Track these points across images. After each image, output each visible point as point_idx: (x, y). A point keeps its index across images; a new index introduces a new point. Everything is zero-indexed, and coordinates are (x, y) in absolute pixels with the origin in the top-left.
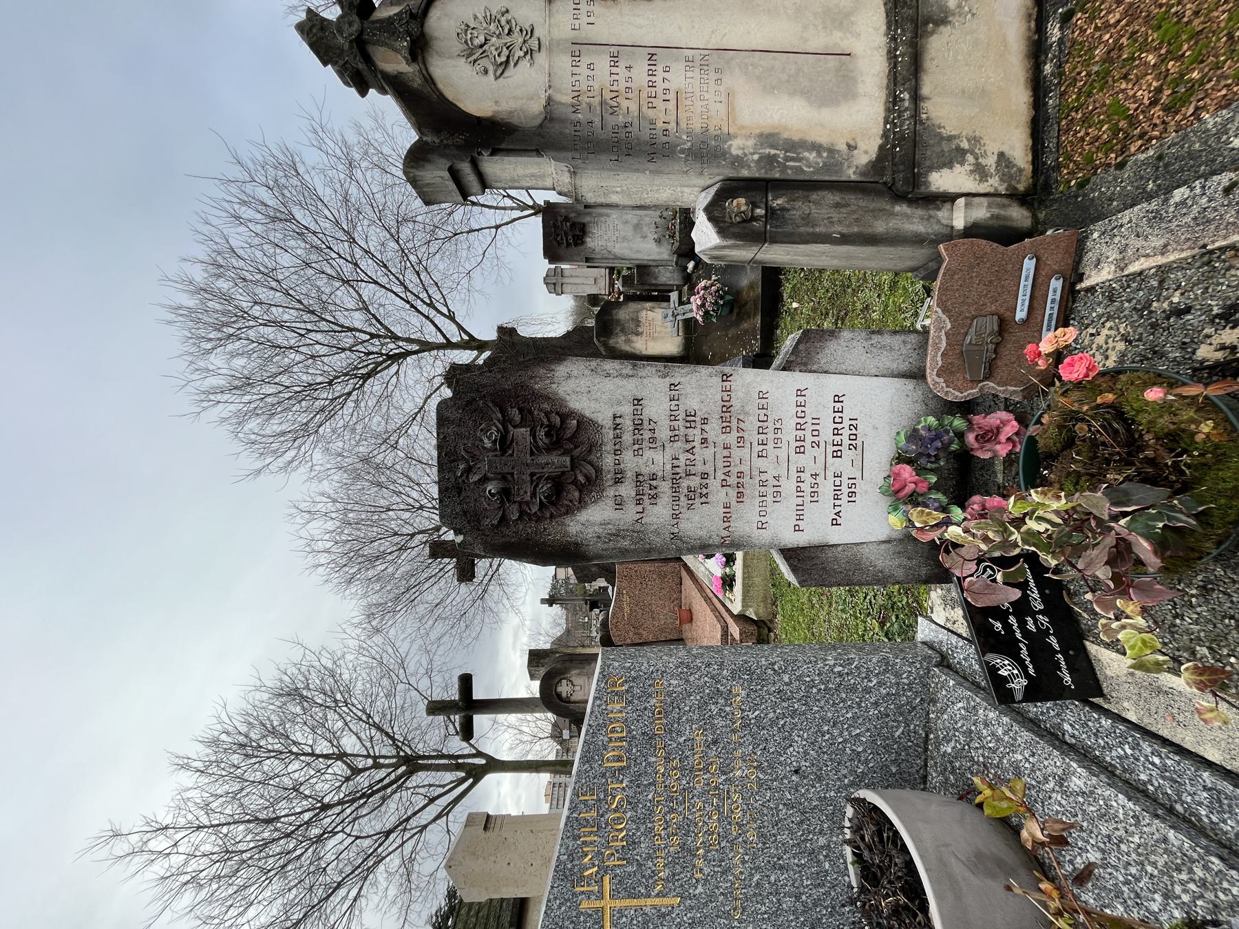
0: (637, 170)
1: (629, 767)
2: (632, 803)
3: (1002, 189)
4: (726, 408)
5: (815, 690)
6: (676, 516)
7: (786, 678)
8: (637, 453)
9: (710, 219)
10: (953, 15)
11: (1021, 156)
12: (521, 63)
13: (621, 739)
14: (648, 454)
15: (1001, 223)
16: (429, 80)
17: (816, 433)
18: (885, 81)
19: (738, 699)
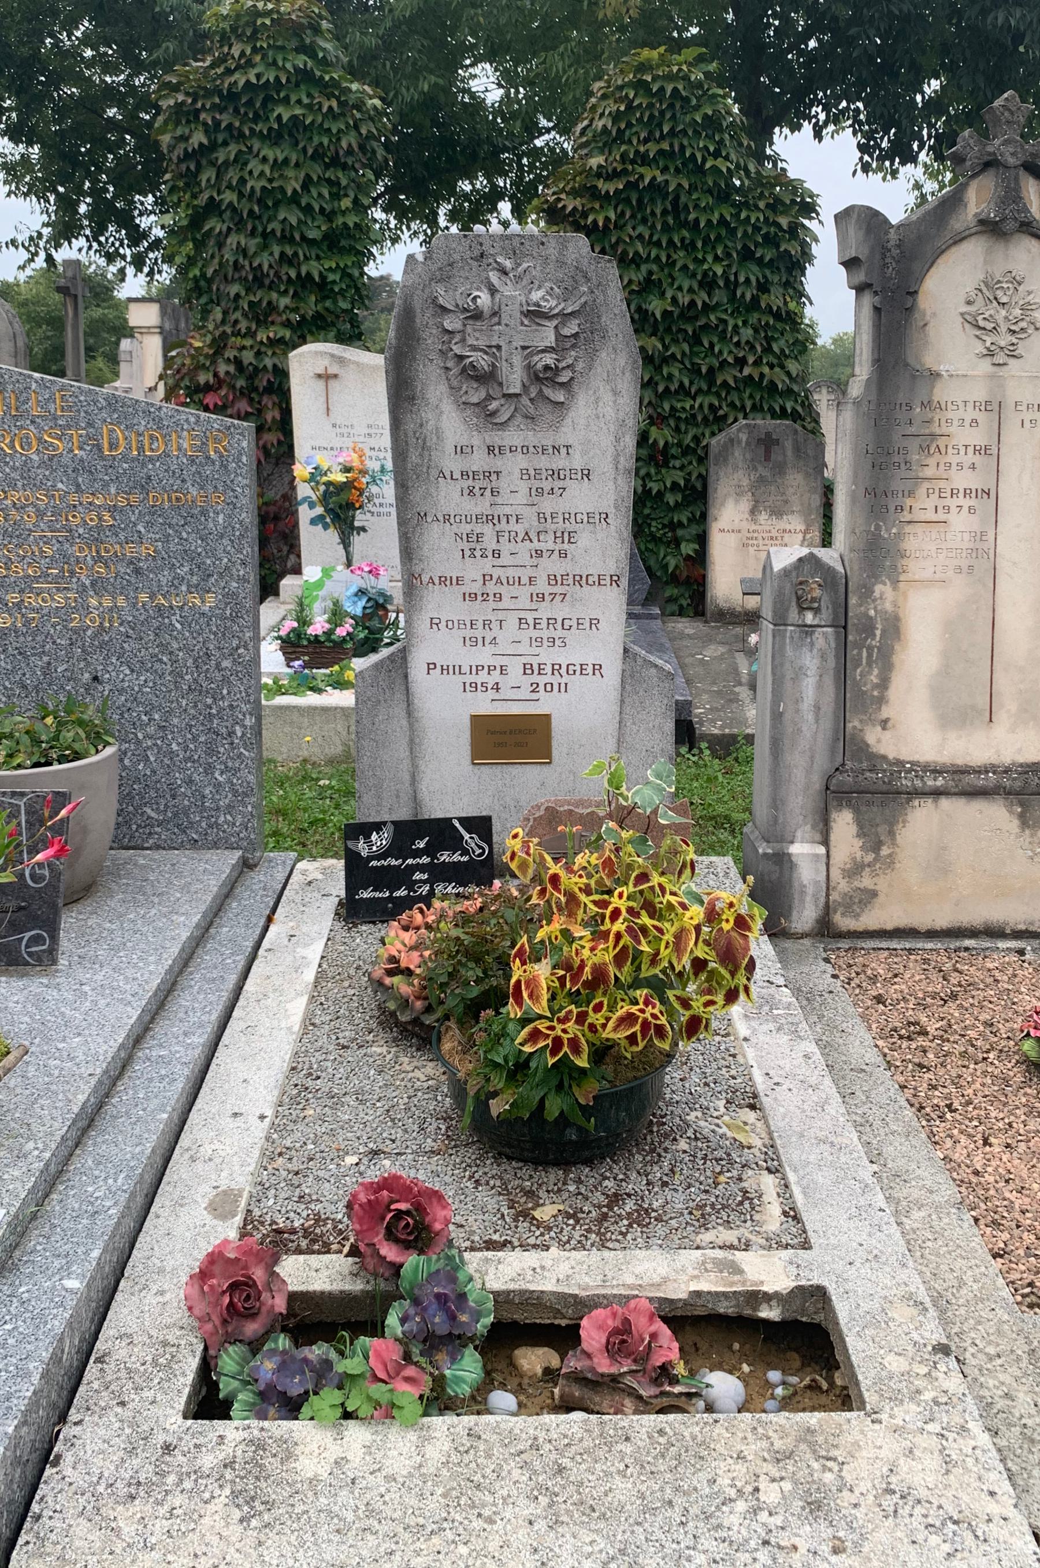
0: (856, 475)
1: (103, 458)
2: (50, 462)
3: (834, 896)
4: (579, 580)
5: (209, 701)
6: (447, 519)
7: (226, 664)
8: (524, 473)
9: (800, 560)
10: (1032, 836)
11: (871, 919)
12: (979, 343)
13: (141, 449)
14: (523, 487)
15: (796, 896)
16: (959, 239)
17: (549, 688)
18: (960, 762)
19: (197, 602)
